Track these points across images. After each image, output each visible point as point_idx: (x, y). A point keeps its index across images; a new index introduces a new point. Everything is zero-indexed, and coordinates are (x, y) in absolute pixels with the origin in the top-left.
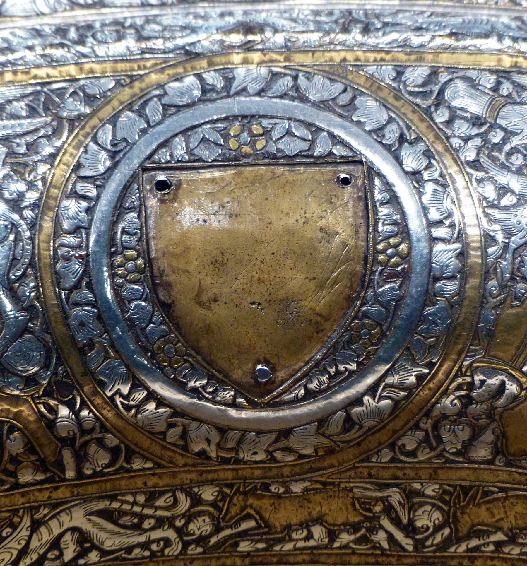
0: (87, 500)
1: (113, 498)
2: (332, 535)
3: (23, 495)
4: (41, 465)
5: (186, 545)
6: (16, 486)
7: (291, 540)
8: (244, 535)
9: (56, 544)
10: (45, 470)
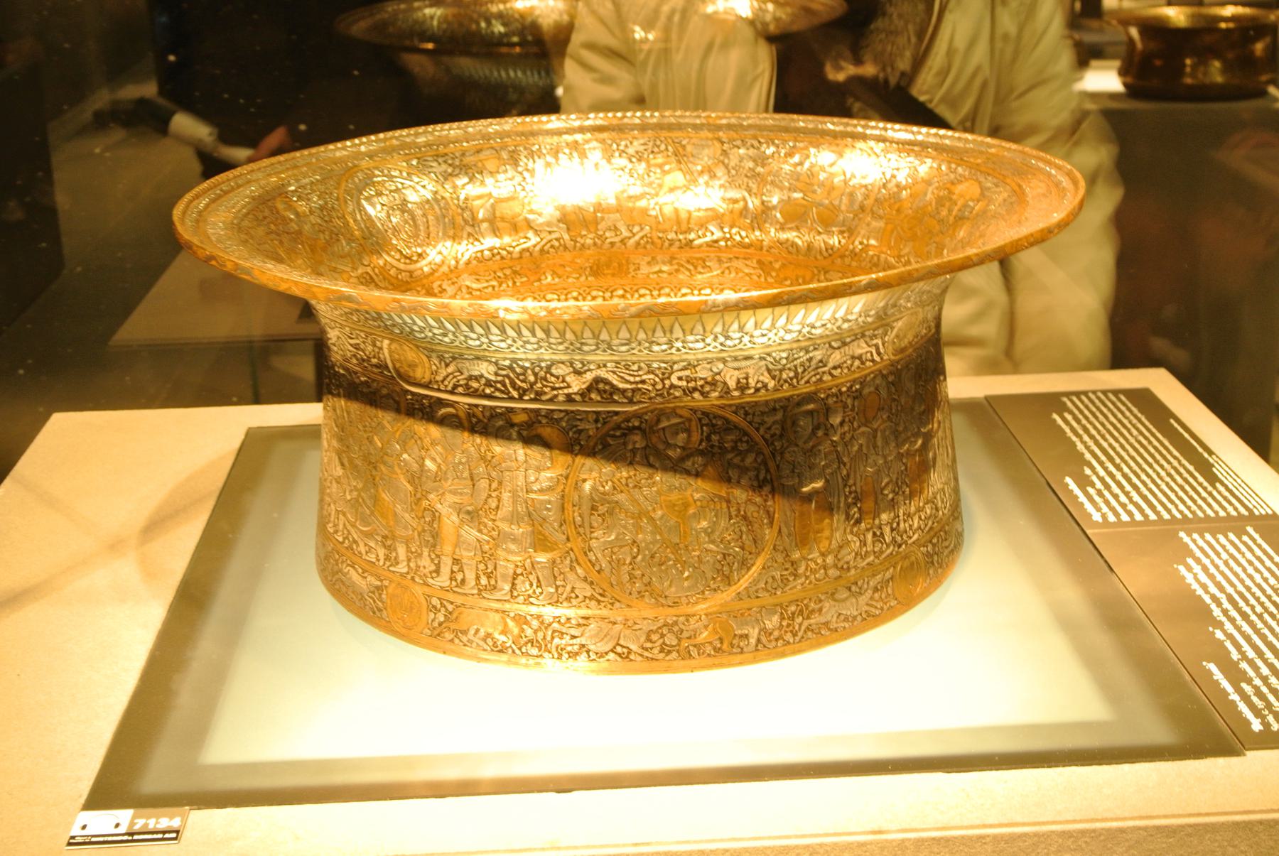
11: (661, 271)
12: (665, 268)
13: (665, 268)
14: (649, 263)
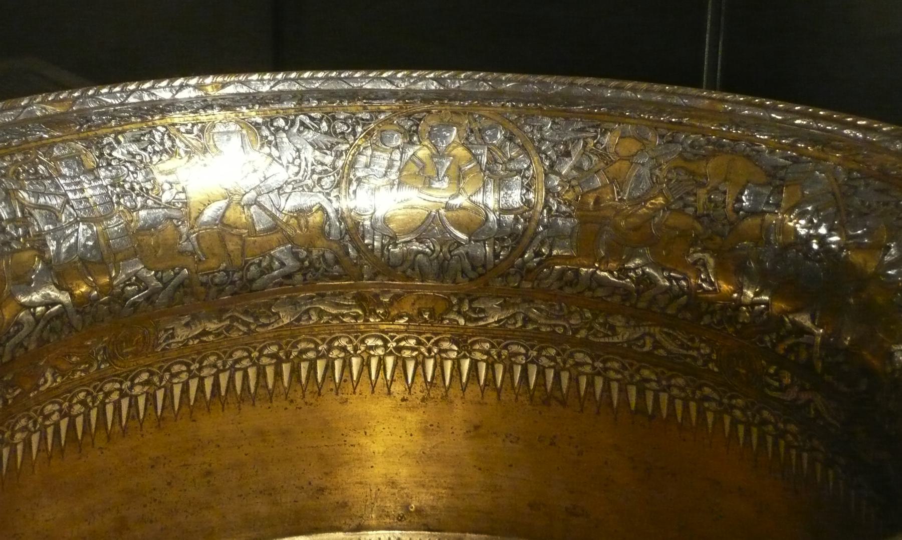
11: (205, 333)
12: (212, 326)
13: (212, 326)
14: (187, 325)
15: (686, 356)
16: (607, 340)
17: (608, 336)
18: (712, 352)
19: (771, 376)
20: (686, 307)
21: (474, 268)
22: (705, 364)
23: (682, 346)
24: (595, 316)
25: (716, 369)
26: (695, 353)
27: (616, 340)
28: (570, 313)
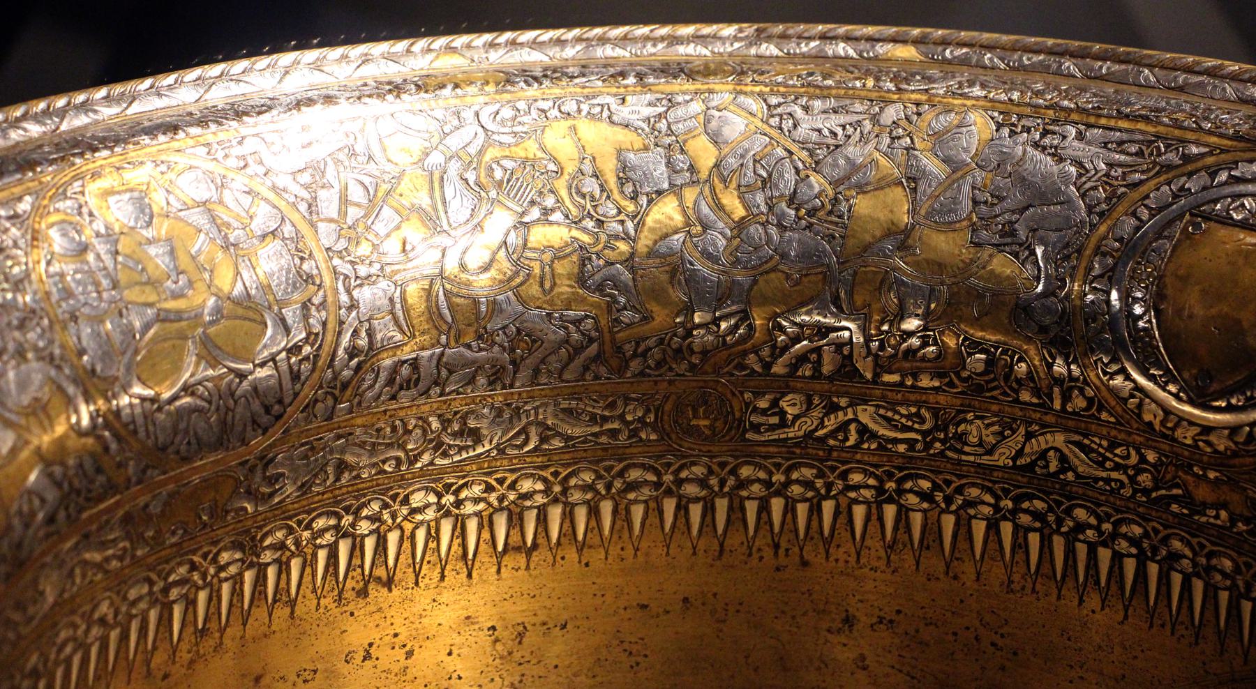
0: (1067, 430)
1: (1086, 436)
2: (1233, 520)
3: (1021, 409)
4: (1036, 392)
5: (1135, 491)
6: (1017, 401)
7: (1205, 515)
8: (1175, 499)
9: (1043, 455)
10: (1039, 397)
15: (595, 435)
16: (464, 455)
17: (466, 448)
18: (648, 411)
19: (764, 412)
20: (598, 358)
21: (268, 410)
22: (634, 433)
23: (593, 419)
24: (445, 423)
25: (653, 437)
26: (616, 426)
27: (480, 450)
28: (408, 432)
